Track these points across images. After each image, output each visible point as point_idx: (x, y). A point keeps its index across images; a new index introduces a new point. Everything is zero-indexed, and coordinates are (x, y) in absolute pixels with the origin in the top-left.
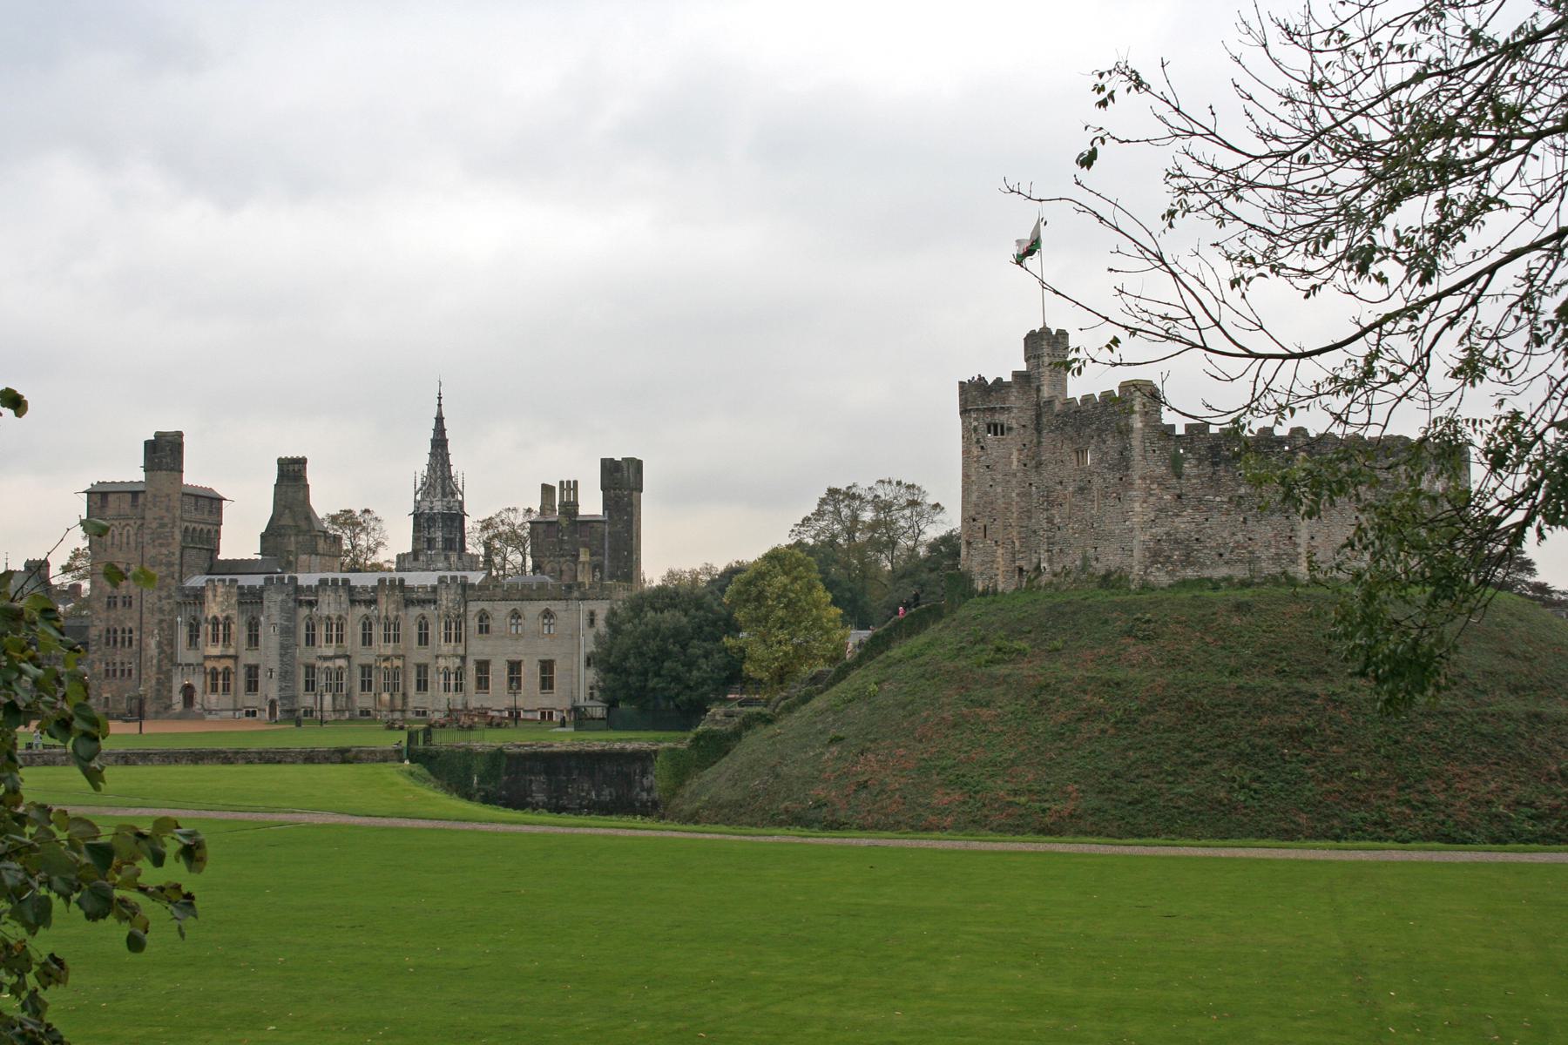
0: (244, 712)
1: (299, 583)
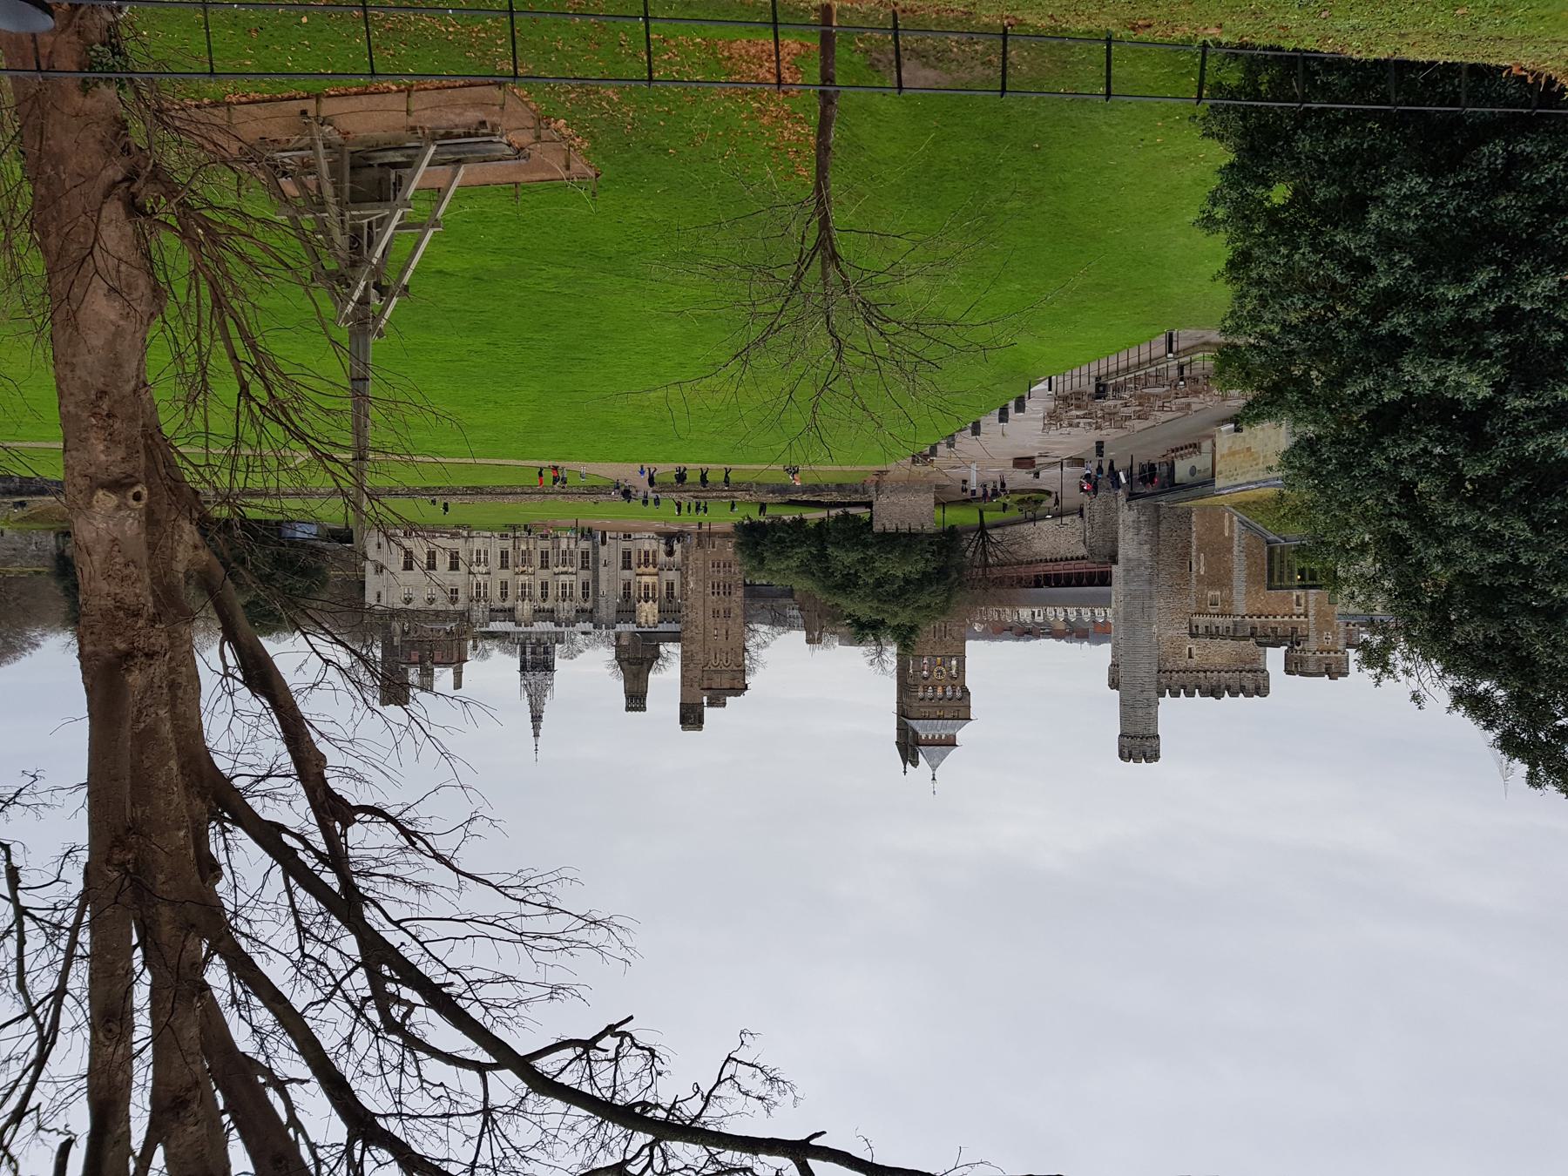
1: (592, 625)
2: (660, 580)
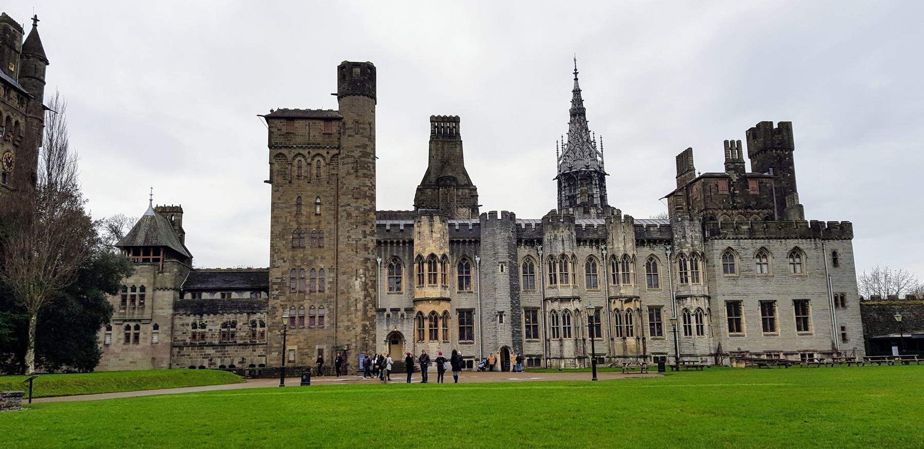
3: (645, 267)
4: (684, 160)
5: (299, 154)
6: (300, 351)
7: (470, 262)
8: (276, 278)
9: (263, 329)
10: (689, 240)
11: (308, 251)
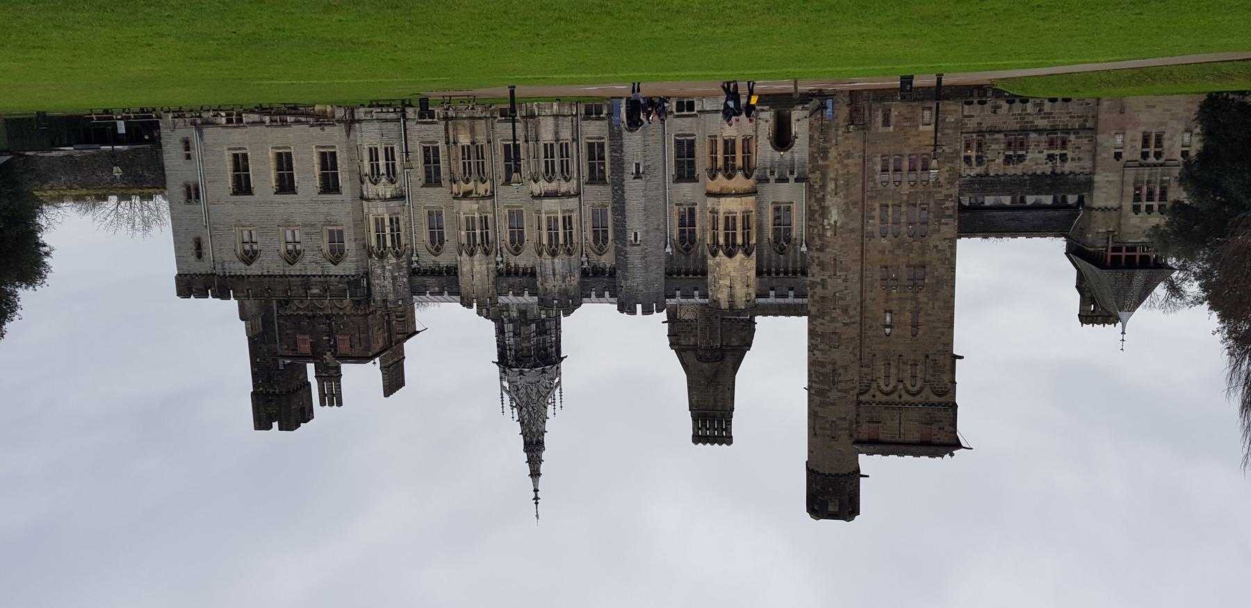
0: (696, 109)
2: (760, 207)
3: (446, 238)
4: (394, 381)
5: (914, 395)
6: (915, 124)
7: (679, 245)
8: (947, 224)
9: (966, 154)
10: (388, 274)
11: (903, 260)
